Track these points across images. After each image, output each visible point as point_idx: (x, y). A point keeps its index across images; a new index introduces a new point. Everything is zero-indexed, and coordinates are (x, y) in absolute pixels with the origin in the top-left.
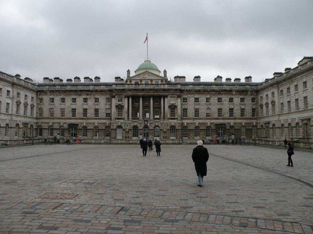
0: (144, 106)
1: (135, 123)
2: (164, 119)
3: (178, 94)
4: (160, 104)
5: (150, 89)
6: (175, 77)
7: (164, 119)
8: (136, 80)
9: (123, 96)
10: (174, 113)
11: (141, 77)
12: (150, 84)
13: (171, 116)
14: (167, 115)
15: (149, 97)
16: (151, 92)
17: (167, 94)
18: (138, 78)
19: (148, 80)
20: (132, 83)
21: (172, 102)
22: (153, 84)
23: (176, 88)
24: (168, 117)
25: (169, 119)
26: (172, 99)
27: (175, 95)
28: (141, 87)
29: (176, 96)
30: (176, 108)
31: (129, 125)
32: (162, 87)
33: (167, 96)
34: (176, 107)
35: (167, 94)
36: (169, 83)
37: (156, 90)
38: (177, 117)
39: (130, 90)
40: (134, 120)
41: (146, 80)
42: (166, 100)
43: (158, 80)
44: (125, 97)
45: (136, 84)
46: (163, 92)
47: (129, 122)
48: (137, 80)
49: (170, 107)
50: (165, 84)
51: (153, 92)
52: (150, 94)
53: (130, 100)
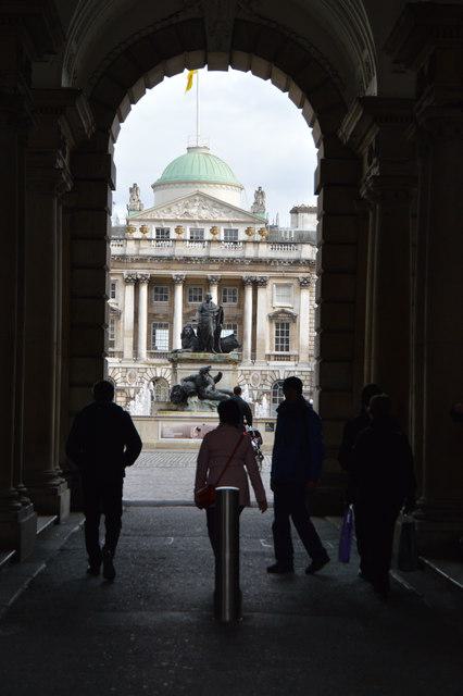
0: (188, 310)
1: (159, 370)
2: (254, 357)
3: (300, 275)
4: (241, 306)
5: (210, 260)
6: (295, 211)
7: (254, 357)
8: (160, 221)
9: (120, 279)
10: (288, 341)
11: (176, 213)
12: (209, 241)
13: (277, 350)
14: (264, 346)
15: (208, 283)
16: (211, 267)
17: (267, 275)
18: (168, 217)
19: (201, 222)
20: (148, 236)
21: (279, 304)
22: (219, 242)
23: (291, 254)
24: (268, 352)
25: (268, 357)
26: (283, 291)
27: (290, 278)
28: (182, 250)
29: (295, 282)
30: (295, 322)
31: (139, 375)
32: (250, 252)
33: (263, 283)
34: (294, 318)
35: (267, 275)
36: (273, 237)
37: (230, 263)
38: (296, 353)
39: (143, 260)
40: (156, 361)
41: (194, 222)
42: (261, 292)
43: (234, 222)
44: (127, 282)
45: (163, 234)
46: (252, 268)
47: (139, 366)
48: (166, 221)
49: (272, 318)
50: (256, 243)
51: (216, 267)
52: (209, 274)
53: (144, 290)
